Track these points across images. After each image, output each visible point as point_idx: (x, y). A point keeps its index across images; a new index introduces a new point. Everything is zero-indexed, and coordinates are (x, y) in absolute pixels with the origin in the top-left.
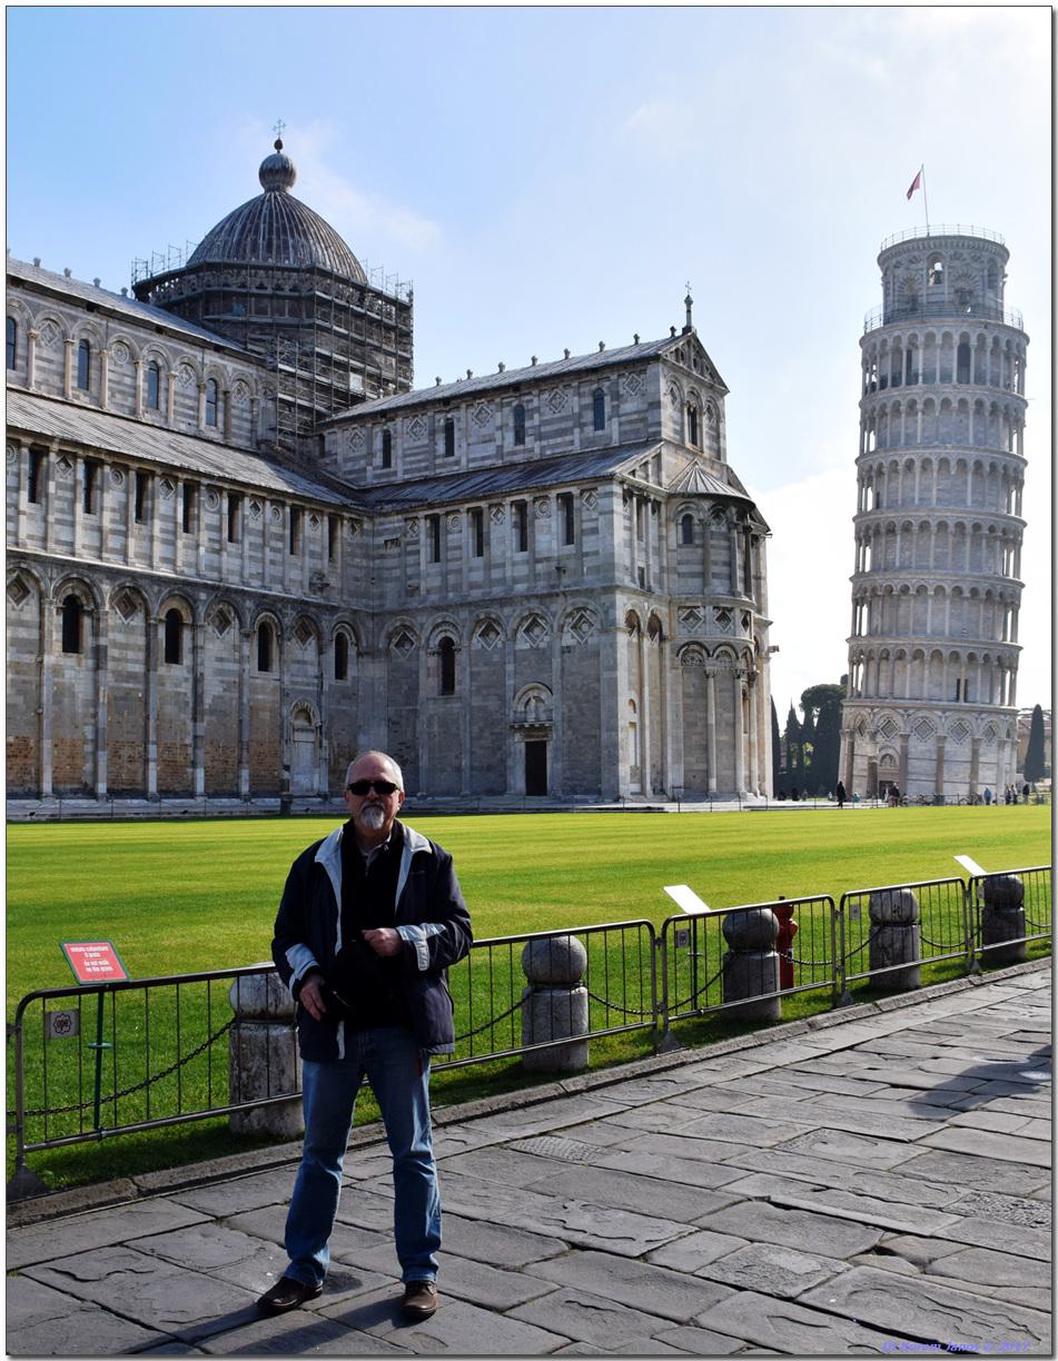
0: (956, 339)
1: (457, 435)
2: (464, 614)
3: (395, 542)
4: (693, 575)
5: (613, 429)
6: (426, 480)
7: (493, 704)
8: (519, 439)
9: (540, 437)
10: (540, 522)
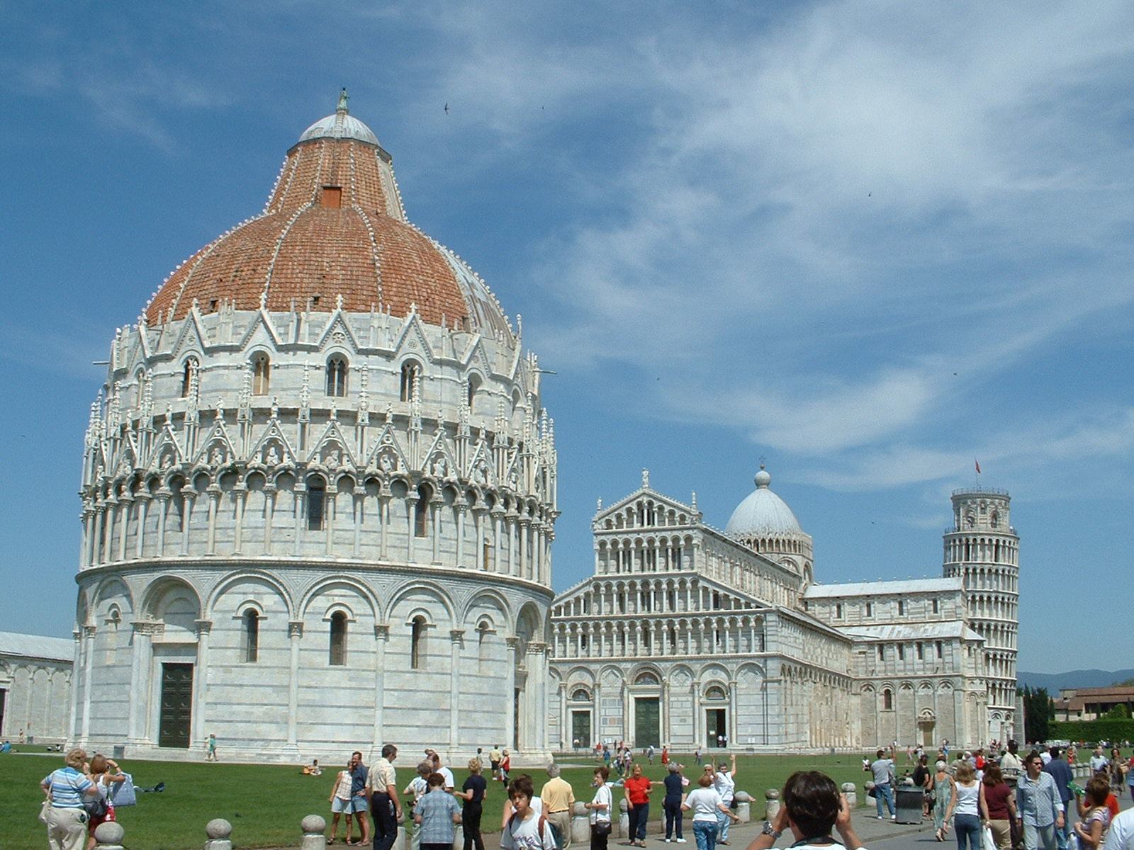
0: (994, 542)
1: (872, 609)
2: (896, 681)
3: (864, 653)
4: (972, 668)
5: (942, 613)
7: (909, 714)
8: (901, 613)
9: (909, 614)
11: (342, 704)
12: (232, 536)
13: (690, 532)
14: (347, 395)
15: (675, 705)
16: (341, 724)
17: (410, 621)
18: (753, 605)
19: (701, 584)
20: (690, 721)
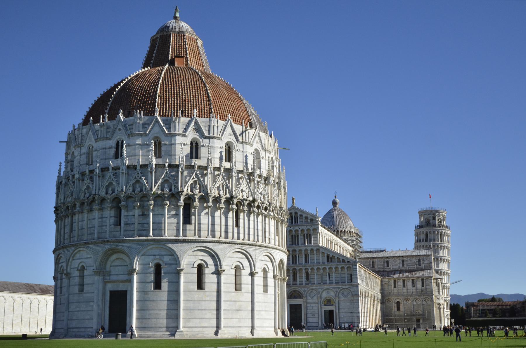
1: (389, 263)
2: (402, 297)
5: (423, 266)
6: (383, 271)
8: (403, 265)
9: (408, 266)
10: (417, 283)
11: (203, 308)
12: (146, 227)
13: (315, 227)
14: (200, 158)
15: (309, 308)
16: (204, 318)
17: (233, 267)
18: (346, 261)
19: (321, 250)
20: (316, 315)
